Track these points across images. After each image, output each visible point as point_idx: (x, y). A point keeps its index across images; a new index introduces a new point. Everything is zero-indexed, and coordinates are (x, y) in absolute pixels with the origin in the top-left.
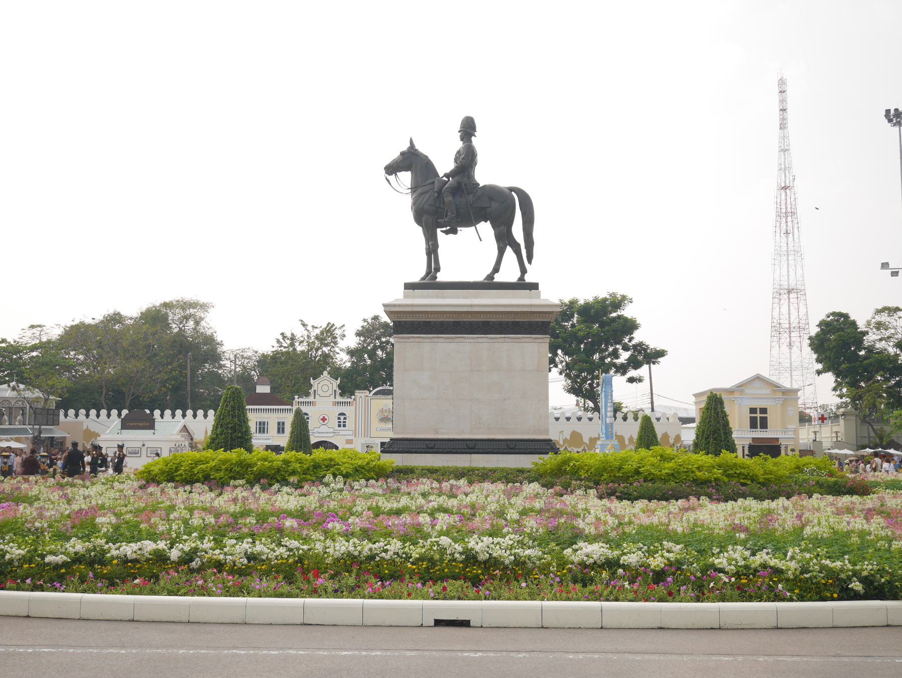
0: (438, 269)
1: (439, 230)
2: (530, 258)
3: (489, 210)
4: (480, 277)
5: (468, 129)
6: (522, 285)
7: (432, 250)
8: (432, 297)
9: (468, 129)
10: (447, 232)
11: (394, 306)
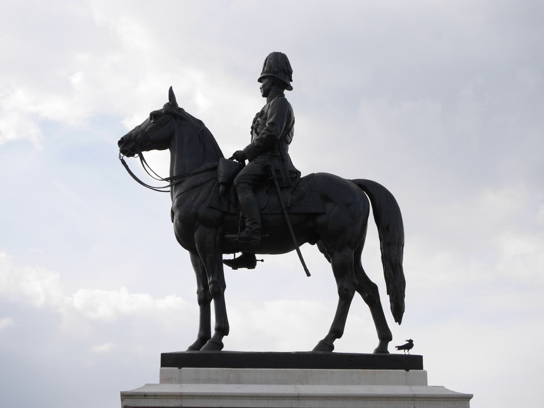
0: (223, 329)
1: (225, 257)
2: (398, 312)
3: (321, 220)
4: (308, 345)
5: (277, 75)
6: (380, 360)
7: (211, 291)
8: (217, 381)
9: (277, 75)
10: (235, 264)
11: (145, 396)
